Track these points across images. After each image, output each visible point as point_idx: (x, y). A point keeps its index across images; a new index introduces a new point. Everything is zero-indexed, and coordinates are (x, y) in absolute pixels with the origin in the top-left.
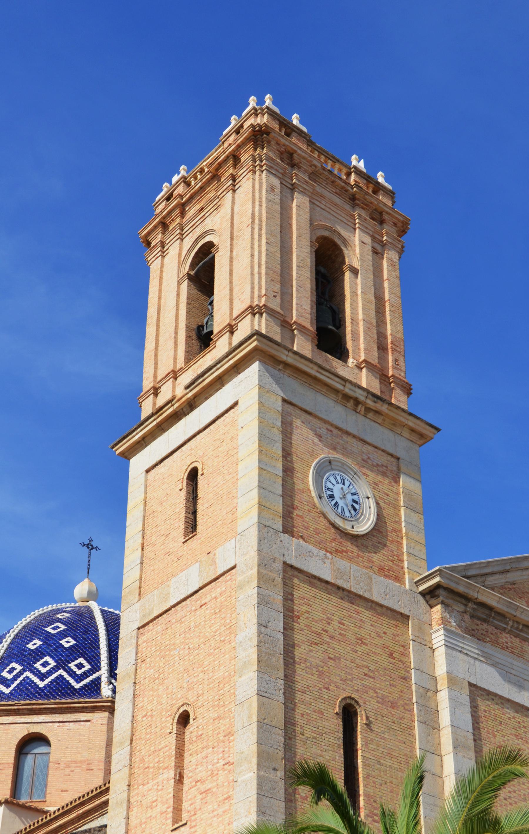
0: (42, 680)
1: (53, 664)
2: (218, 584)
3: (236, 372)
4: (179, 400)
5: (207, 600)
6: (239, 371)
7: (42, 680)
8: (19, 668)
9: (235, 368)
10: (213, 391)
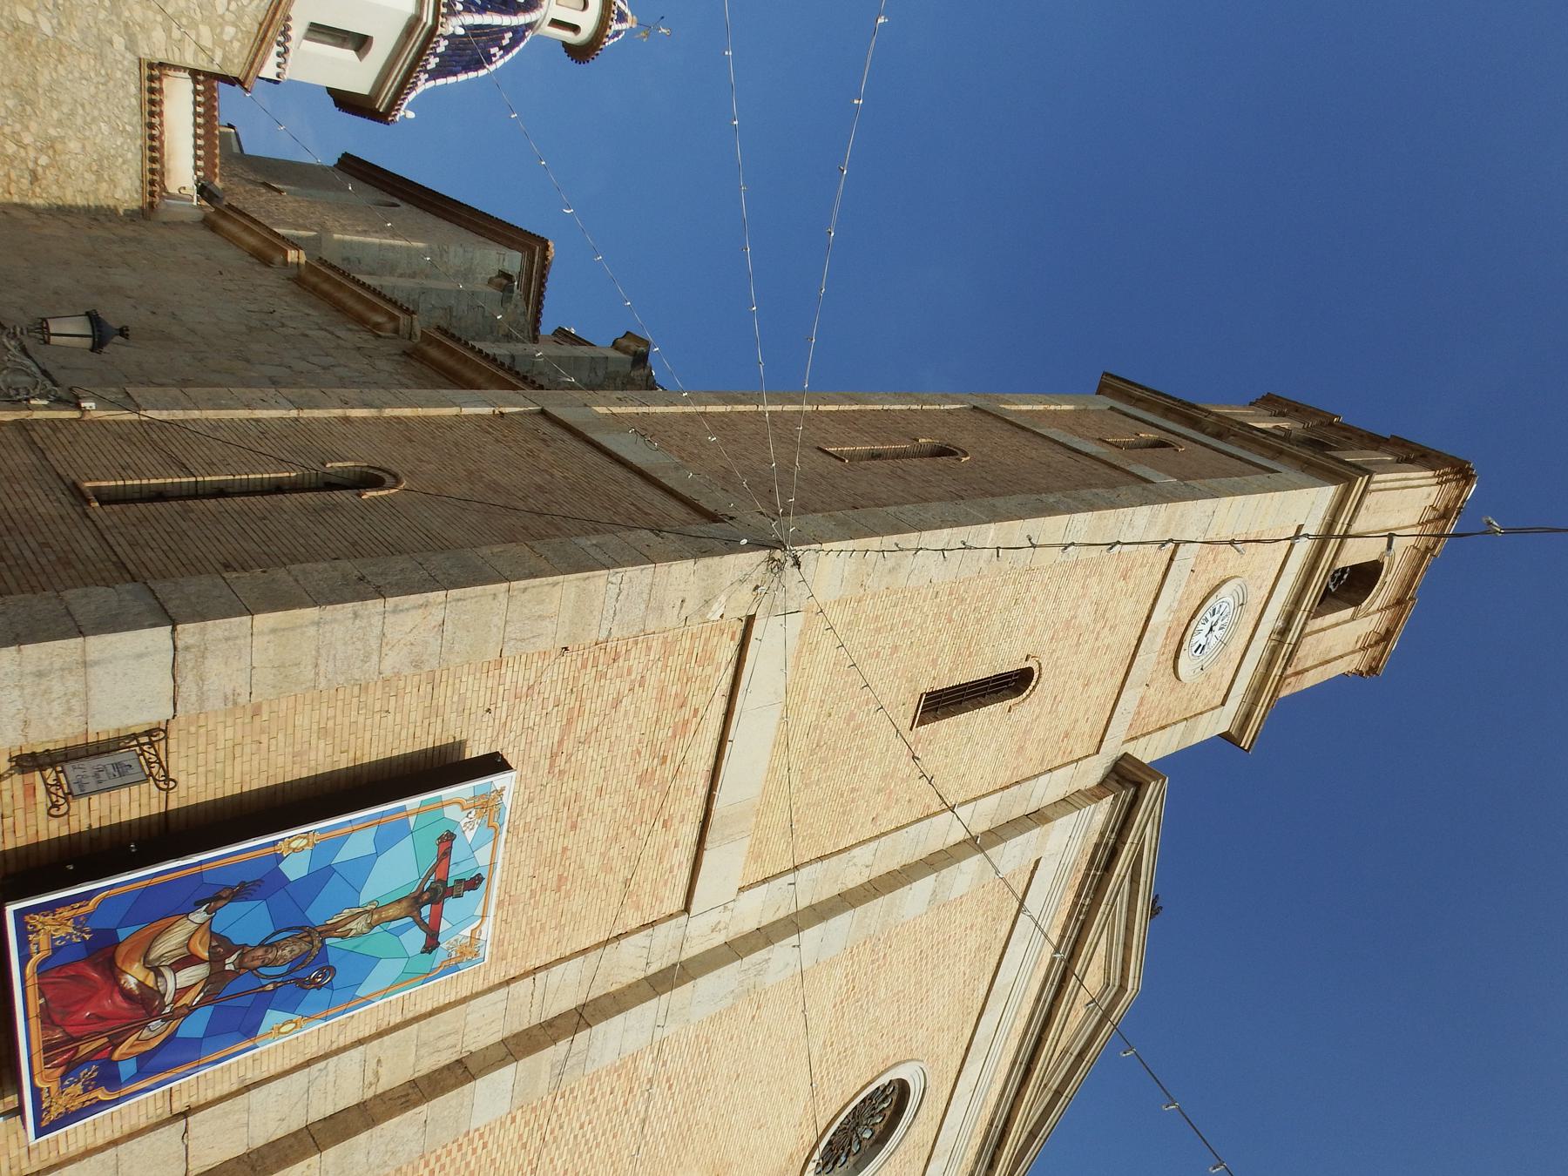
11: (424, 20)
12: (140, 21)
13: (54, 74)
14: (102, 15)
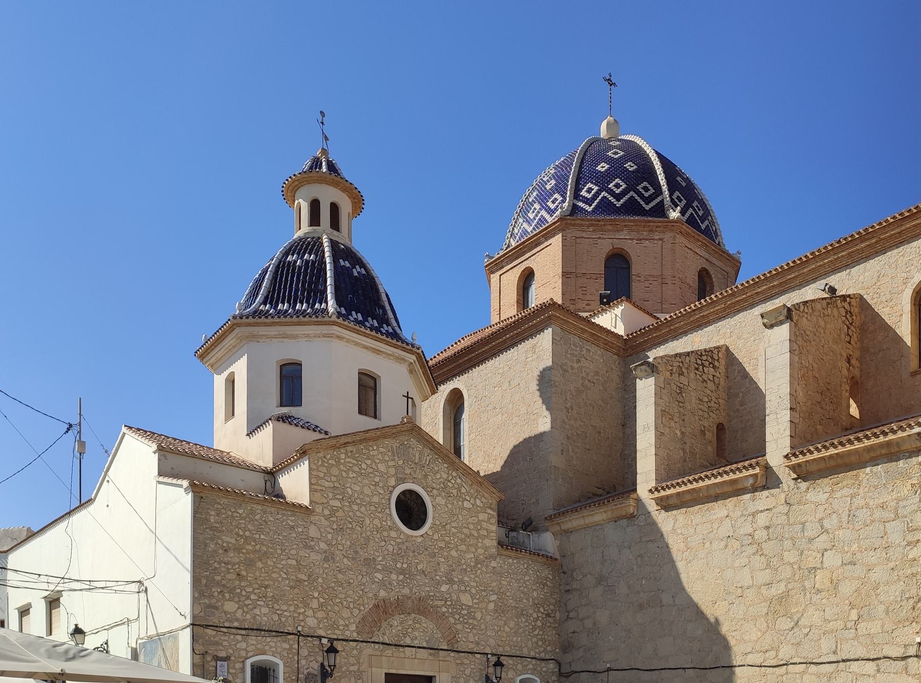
0: (618, 200)
1: (624, 186)
7: (618, 200)
8: (596, 188)
11: (413, 362)
12: (483, 551)
13: (511, 598)
14: (484, 569)
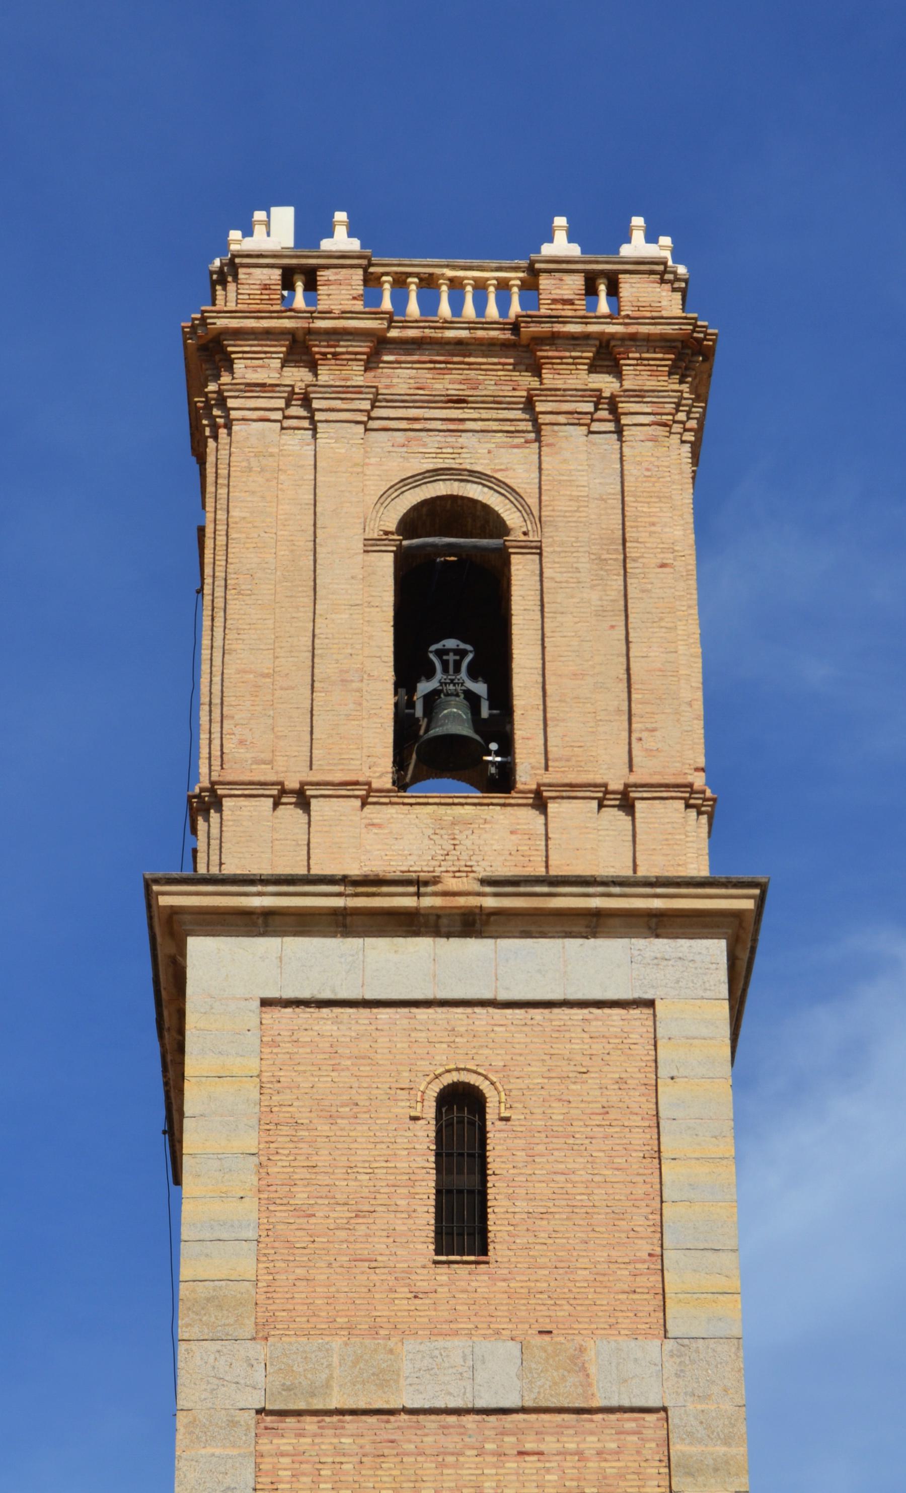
2: (588, 1425)
3: (650, 928)
4: (445, 894)
5: (543, 1447)
6: (659, 931)
9: (654, 920)
10: (559, 929)
